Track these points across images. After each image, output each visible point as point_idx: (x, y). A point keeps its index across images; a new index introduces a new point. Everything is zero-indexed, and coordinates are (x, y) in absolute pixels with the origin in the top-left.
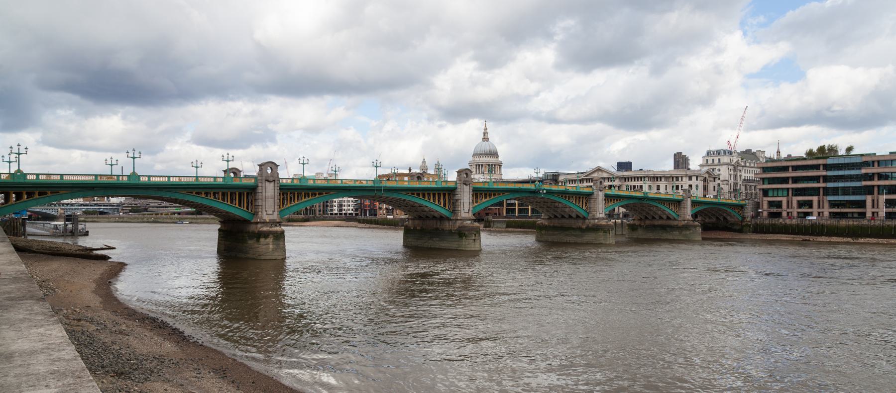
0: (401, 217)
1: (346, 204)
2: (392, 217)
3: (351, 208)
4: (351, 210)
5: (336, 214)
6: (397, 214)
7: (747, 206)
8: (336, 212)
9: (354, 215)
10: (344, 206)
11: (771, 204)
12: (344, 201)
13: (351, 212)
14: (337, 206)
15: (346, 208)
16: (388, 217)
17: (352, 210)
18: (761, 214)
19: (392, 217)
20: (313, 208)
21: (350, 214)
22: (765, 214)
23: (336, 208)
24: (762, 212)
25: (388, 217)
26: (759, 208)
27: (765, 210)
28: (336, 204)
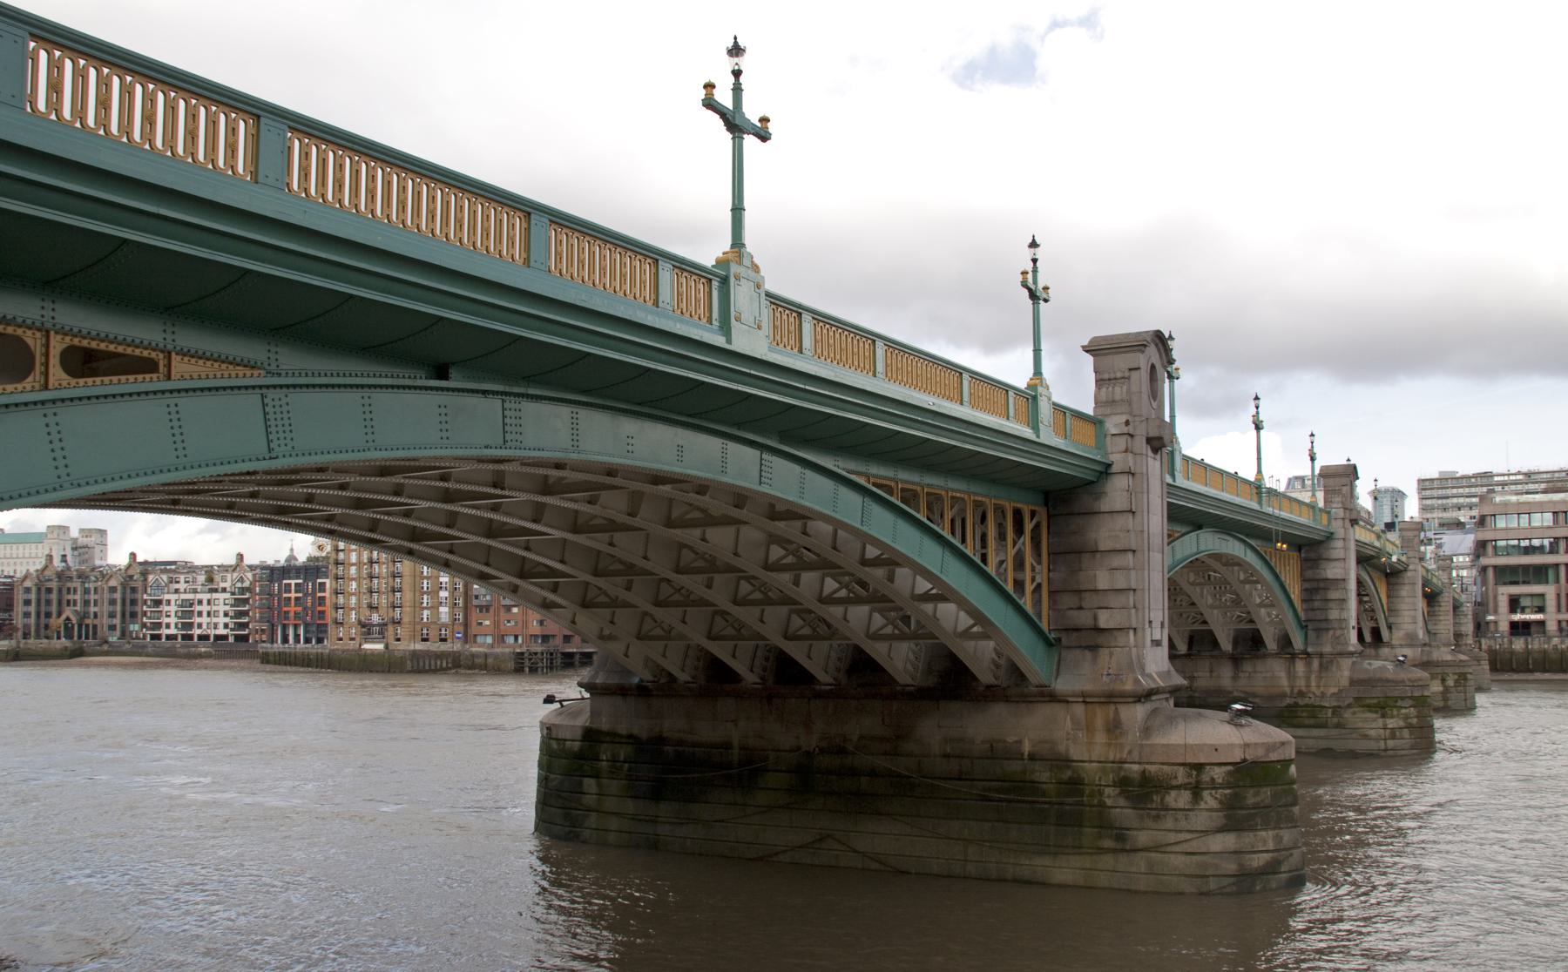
0: (412, 647)
1: (205, 608)
2: (380, 646)
3: (222, 620)
4: (221, 626)
5: (169, 637)
6: (398, 640)
7: (1465, 609)
8: (173, 631)
9: (231, 640)
10: (200, 614)
11: (1514, 604)
12: (200, 602)
13: (222, 631)
14: (173, 614)
15: (204, 620)
16: (366, 646)
17: (226, 626)
18: (1492, 627)
19: (380, 646)
20: (87, 621)
21: (218, 638)
22: (1504, 627)
23: (173, 620)
24: (1496, 622)
25: (366, 646)
26: (1487, 612)
27: (1502, 618)
28: (173, 608)
